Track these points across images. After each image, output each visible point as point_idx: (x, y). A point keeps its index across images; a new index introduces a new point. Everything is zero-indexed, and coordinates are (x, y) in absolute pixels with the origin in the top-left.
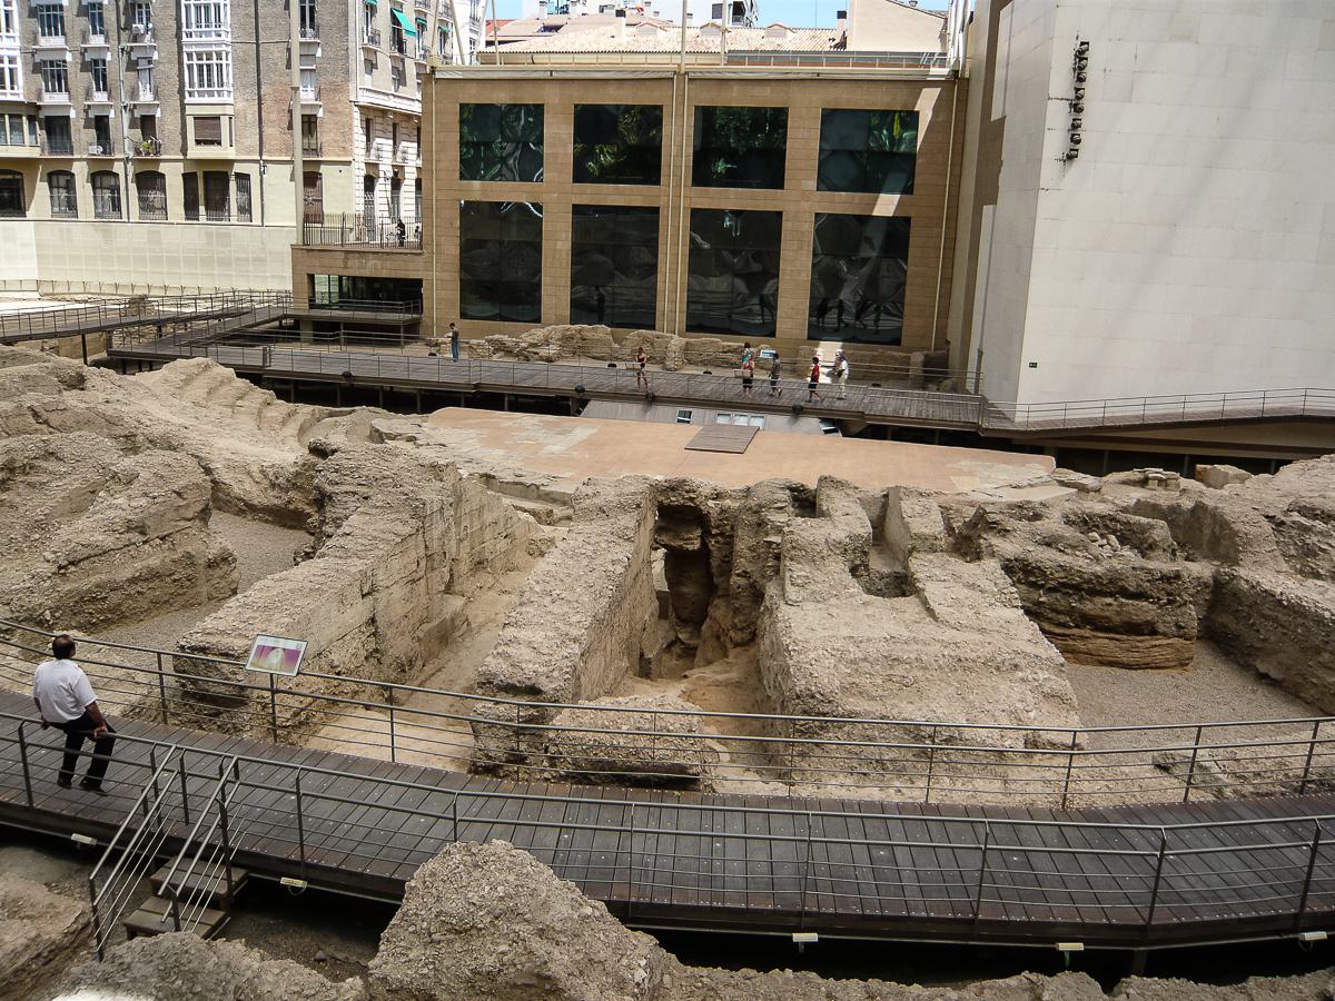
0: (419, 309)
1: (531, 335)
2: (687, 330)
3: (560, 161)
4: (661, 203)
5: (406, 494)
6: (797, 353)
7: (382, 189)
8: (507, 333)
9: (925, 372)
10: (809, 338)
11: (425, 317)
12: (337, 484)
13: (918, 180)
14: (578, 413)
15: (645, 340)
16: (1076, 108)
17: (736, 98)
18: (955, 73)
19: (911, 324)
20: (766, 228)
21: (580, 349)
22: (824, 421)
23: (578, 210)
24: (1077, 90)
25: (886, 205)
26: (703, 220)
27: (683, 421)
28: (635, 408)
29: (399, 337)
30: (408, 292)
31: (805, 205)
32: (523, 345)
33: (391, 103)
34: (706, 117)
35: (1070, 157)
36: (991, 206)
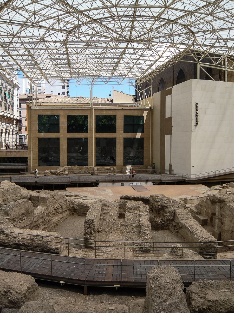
0: (27, 165)
1: (60, 169)
2: (96, 165)
3: (64, 128)
4: (88, 137)
5: (181, 204)
6: (122, 169)
7: (3, 135)
8: (49, 170)
9: (153, 170)
10: (124, 165)
11: (29, 166)
12: (167, 203)
13: (144, 130)
14: (97, 186)
15: (87, 168)
16: (197, 116)
17: (104, 113)
18: (151, 108)
19: (145, 160)
20: (113, 142)
21: (72, 171)
22: (153, 182)
23: (68, 139)
24: (197, 112)
25: (139, 135)
26: (98, 141)
27: (122, 186)
28: (110, 184)
29: (7, 173)
30: (24, 160)
31: (121, 136)
32: (59, 172)
33: (5, 114)
34: (98, 118)
35: (197, 125)
36: (169, 135)
